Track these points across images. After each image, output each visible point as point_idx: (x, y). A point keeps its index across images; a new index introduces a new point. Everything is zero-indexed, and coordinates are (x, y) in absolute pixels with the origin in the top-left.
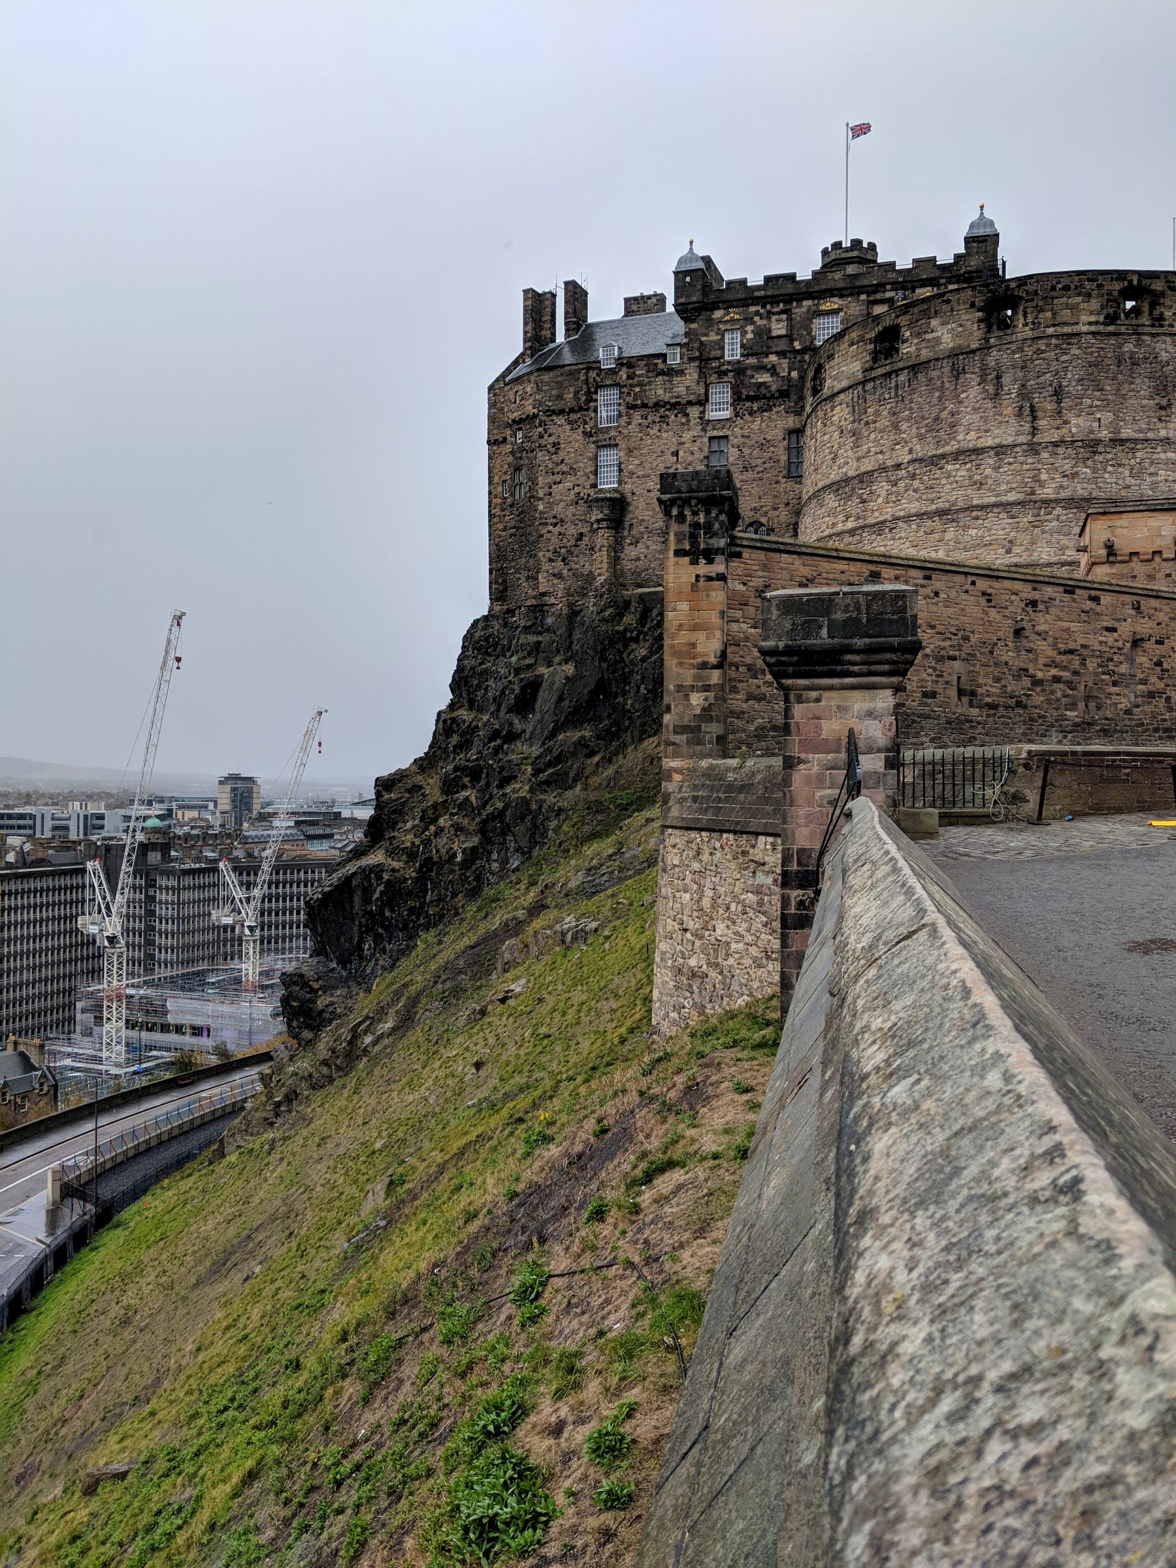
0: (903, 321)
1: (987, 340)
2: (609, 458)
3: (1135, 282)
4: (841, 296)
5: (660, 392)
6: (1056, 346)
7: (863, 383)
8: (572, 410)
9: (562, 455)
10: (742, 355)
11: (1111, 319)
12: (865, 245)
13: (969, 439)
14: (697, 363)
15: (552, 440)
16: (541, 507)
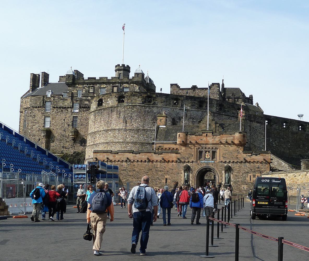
0: (104, 97)
1: (118, 105)
2: (48, 120)
3: (149, 95)
4: (106, 84)
5: (61, 104)
6: (132, 108)
7: (96, 111)
8: (39, 107)
9: (36, 118)
10: (82, 96)
11: (143, 103)
12: (126, 66)
13: (113, 126)
14: (71, 98)
15: (33, 114)
16: (29, 131)
